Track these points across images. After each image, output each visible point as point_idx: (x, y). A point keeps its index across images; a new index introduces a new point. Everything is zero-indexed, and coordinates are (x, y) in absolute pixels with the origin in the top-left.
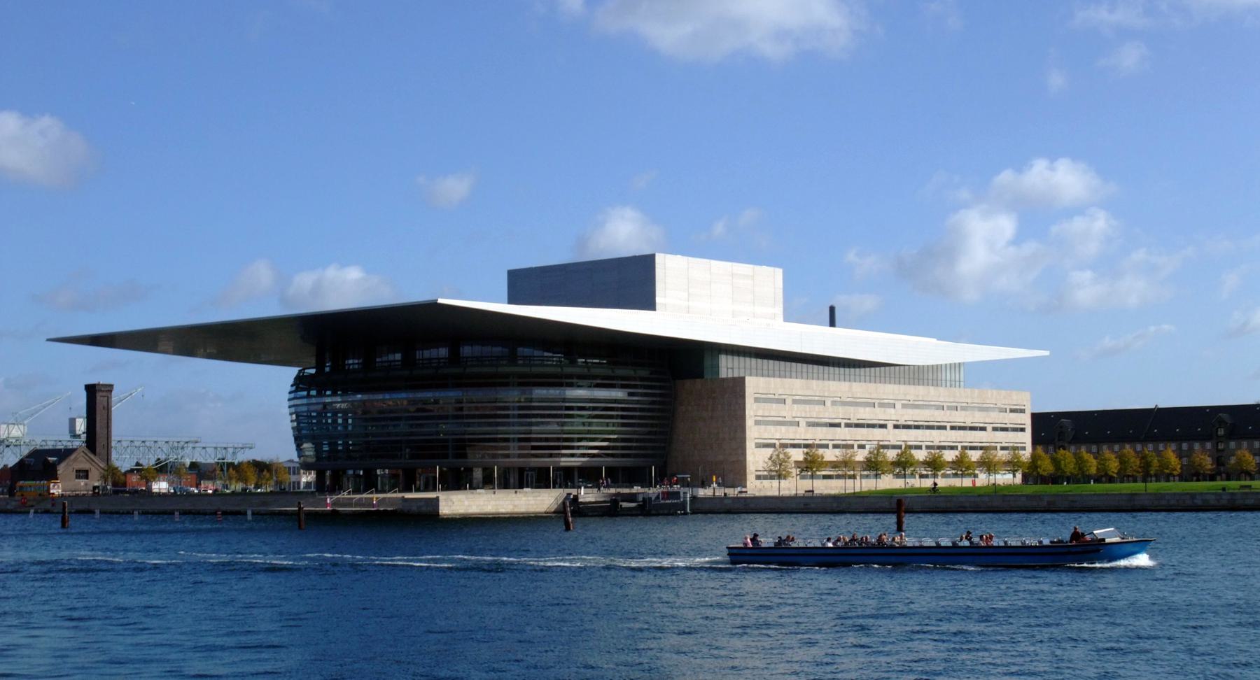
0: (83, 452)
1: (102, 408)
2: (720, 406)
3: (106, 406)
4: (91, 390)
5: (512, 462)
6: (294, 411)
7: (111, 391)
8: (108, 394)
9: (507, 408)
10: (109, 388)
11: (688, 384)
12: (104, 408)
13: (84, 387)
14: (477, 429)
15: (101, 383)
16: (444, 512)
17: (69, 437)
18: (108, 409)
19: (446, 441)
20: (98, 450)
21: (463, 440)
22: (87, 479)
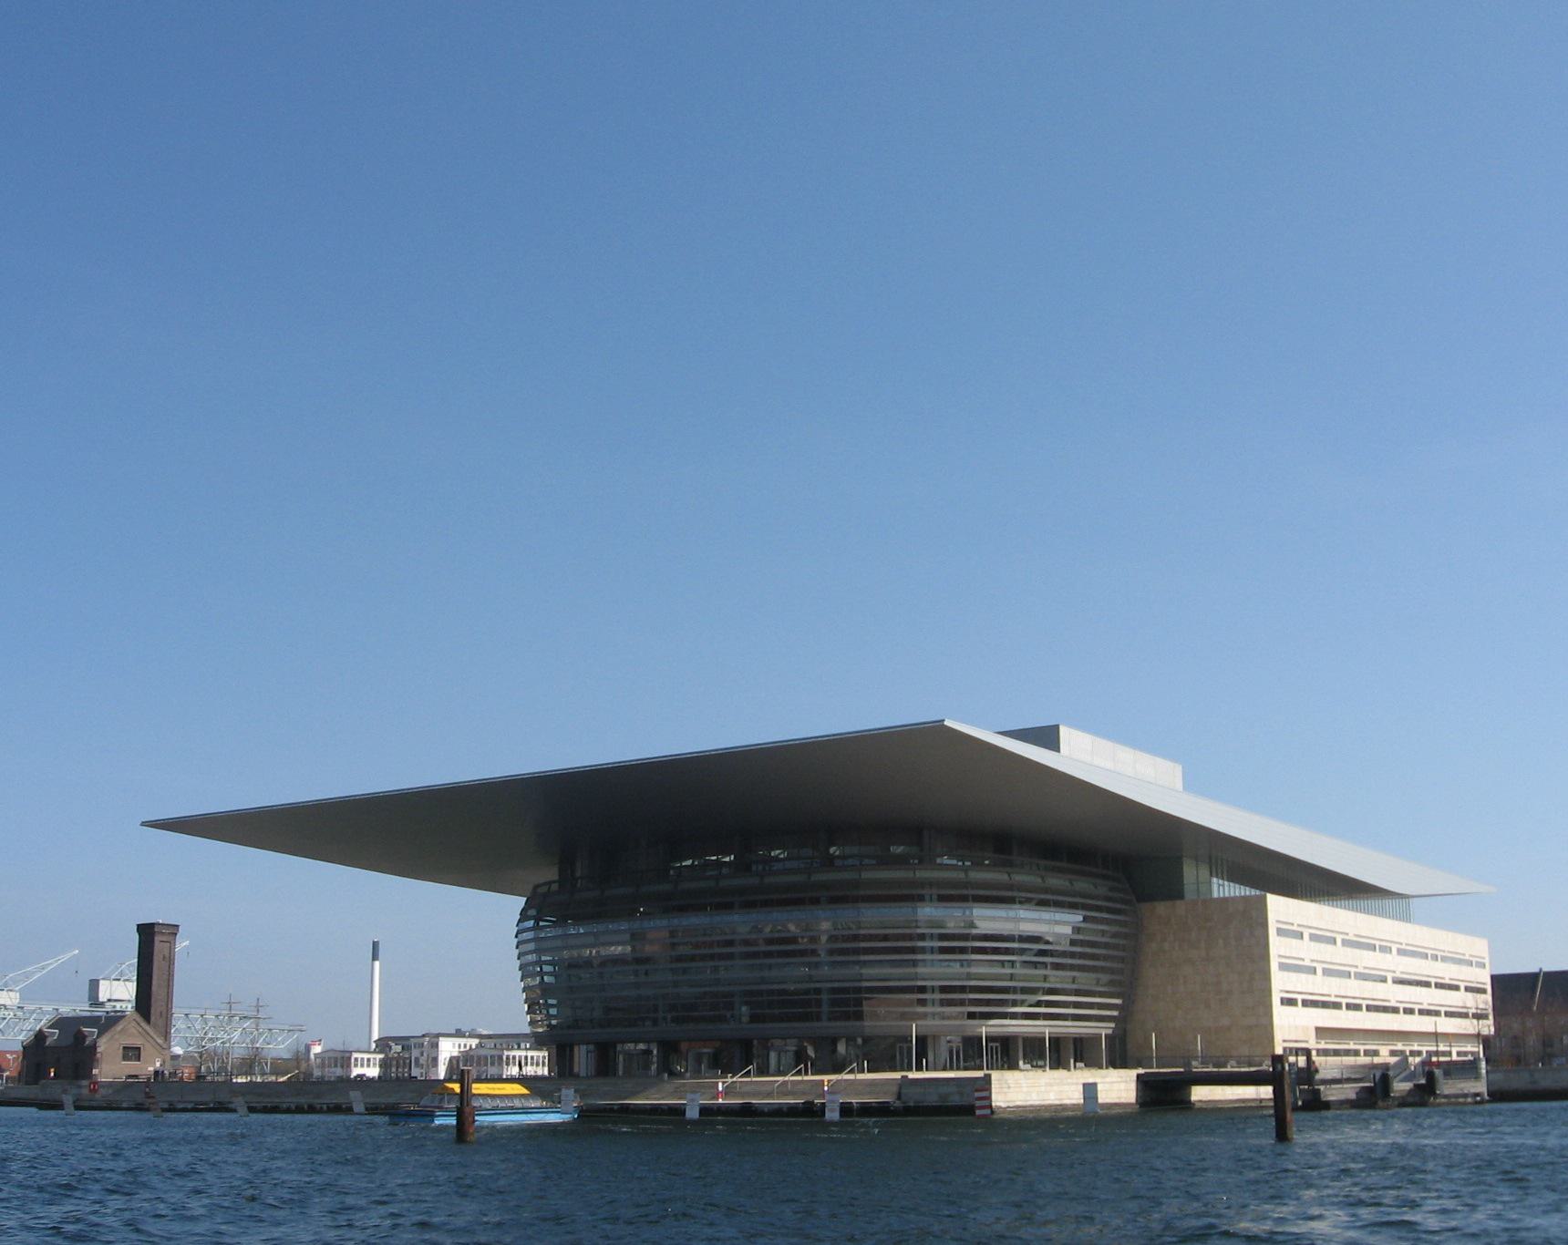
0: (134, 1020)
1: (161, 960)
2: (1221, 941)
3: (167, 955)
4: (147, 933)
5: (926, 1026)
6: (533, 948)
7: (176, 934)
8: (170, 938)
9: (922, 937)
10: (173, 930)
11: (1162, 908)
12: (164, 957)
13: (136, 928)
14: (873, 973)
15: (161, 922)
16: (998, 1104)
17: (88, 1005)
18: (170, 960)
19: (818, 991)
20: (153, 1019)
21: (859, 990)
22: (139, 1060)
